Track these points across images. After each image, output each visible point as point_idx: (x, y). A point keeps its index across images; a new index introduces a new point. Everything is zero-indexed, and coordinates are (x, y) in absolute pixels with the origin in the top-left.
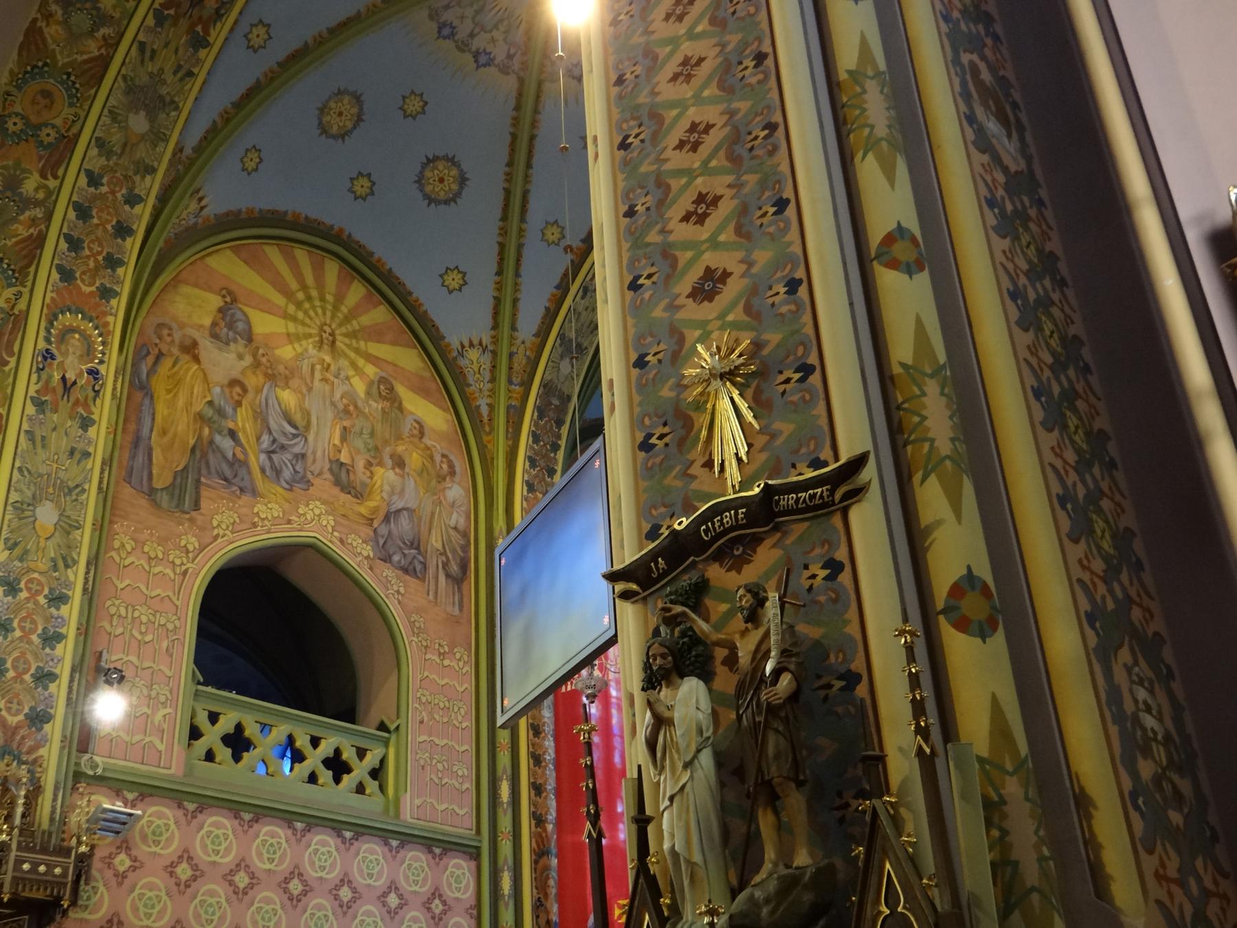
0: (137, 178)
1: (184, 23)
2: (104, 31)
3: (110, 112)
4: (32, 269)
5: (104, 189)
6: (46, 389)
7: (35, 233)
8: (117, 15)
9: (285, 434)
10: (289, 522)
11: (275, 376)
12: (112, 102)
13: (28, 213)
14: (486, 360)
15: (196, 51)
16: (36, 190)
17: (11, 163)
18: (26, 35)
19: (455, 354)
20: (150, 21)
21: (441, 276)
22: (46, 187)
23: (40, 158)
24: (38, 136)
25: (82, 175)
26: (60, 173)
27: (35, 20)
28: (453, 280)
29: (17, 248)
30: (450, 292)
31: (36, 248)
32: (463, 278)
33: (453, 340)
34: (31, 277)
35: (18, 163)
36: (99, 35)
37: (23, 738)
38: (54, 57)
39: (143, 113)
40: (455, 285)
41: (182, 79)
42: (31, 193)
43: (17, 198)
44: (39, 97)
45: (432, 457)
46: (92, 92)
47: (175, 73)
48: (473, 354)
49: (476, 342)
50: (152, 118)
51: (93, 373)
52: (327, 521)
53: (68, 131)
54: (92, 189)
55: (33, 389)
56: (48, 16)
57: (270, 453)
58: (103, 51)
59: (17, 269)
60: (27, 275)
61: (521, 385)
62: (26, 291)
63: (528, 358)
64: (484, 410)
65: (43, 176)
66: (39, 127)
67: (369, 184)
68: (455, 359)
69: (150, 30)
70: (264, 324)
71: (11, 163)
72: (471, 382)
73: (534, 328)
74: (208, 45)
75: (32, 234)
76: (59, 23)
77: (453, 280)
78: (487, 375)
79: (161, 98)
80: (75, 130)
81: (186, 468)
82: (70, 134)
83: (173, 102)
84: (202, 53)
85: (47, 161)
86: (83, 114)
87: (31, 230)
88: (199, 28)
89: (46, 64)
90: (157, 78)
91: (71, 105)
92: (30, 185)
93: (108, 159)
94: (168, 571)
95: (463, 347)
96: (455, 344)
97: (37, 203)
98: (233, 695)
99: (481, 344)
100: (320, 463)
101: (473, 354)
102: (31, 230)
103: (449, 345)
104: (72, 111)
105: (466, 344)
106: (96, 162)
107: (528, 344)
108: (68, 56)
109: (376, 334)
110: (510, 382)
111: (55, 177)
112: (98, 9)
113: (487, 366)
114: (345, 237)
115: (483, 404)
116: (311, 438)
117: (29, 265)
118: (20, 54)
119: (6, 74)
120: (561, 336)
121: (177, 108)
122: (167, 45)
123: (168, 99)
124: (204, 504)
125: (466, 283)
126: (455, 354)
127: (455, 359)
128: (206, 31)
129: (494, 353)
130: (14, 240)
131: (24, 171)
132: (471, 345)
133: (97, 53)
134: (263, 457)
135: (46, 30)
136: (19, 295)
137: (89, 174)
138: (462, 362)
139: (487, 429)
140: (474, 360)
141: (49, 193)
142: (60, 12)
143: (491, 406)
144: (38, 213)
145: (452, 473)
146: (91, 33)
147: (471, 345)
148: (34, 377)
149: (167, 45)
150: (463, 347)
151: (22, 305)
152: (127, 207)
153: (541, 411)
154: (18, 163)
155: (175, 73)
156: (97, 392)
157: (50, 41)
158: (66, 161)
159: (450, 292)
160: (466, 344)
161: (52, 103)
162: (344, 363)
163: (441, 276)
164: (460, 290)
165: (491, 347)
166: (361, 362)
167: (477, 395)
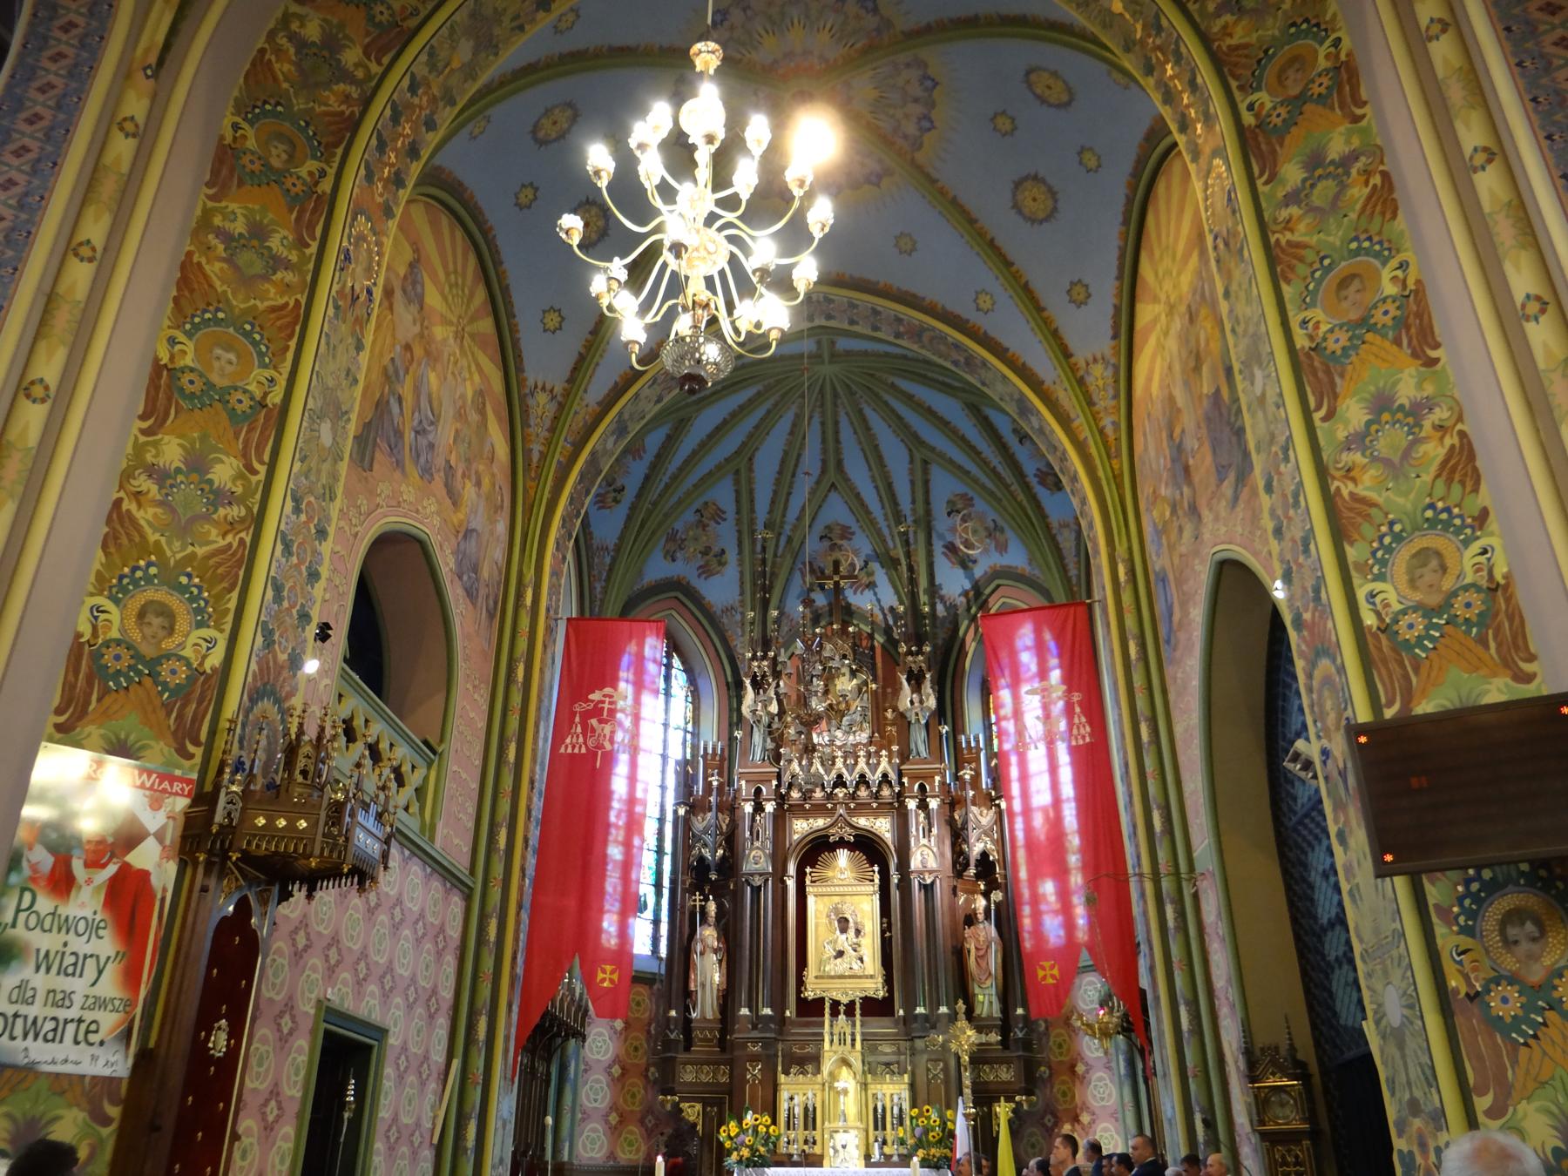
0: (441, 104)
3: (452, 26)
4: (340, 151)
6: (341, 293)
7: (347, 113)
9: (427, 418)
10: (417, 512)
11: (432, 356)
12: (457, 17)
14: (553, 407)
15: (537, 10)
16: (357, 65)
17: (335, 21)
19: (527, 391)
21: (544, 312)
23: (368, 34)
24: (371, 9)
25: (408, 77)
26: (386, 60)
28: (552, 320)
30: (545, 331)
32: (560, 323)
33: (532, 376)
34: (338, 159)
37: (284, 681)
39: (472, 43)
40: (551, 325)
41: (513, 29)
42: (350, 66)
43: (334, 63)
45: (494, 485)
48: (542, 398)
49: (548, 387)
50: (476, 52)
51: (369, 292)
52: (436, 521)
53: (403, 20)
54: (409, 95)
55: (336, 287)
57: (417, 432)
59: (324, 141)
60: (334, 155)
61: (573, 444)
62: (331, 172)
63: (586, 422)
64: (535, 457)
65: (367, 54)
67: (531, 197)
68: (526, 395)
70: (433, 298)
71: (335, 21)
72: (532, 423)
73: (600, 397)
75: (343, 113)
77: (552, 320)
78: (548, 423)
80: (412, 23)
81: (370, 422)
83: (497, 46)
84: (541, 14)
87: (343, 107)
92: (351, 56)
93: (430, 72)
94: (347, 528)
95: (536, 387)
96: (530, 382)
97: (352, 80)
98: (357, 678)
99: (551, 391)
100: (440, 462)
101: (542, 398)
102: (343, 107)
103: (525, 380)
105: (540, 385)
106: (421, 70)
107: (590, 409)
109: (483, 346)
110: (566, 440)
111: (379, 63)
113: (550, 415)
114: (490, 237)
115: (536, 448)
116: (440, 429)
117: (337, 145)
120: (620, 413)
121: (496, 54)
123: (494, 42)
124: (376, 466)
125: (560, 328)
126: (527, 391)
127: (526, 395)
129: (561, 406)
130: (323, 108)
131: (346, 37)
132: (543, 389)
134: (413, 434)
136: (323, 174)
137: (413, 76)
138: (531, 402)
139: (533, 475)
140: (542, 405)
141: (369, 77)
143: (543, 456)
144: (354, 92)
145: (502, 507)
147: (543, 389)
148: (337, 274)
150: (536, 387)
151: (326, 186)
152: (424, 129)
153: (582, 475)
155: (512, 20)
156: (369, 315)
159: (545, 331)
160: (540, 385)
162: (464, 362)
163: (544, 312)
164: (554, 332)
165: (559, 398)
166: (473, 368)
167: (533, 438)
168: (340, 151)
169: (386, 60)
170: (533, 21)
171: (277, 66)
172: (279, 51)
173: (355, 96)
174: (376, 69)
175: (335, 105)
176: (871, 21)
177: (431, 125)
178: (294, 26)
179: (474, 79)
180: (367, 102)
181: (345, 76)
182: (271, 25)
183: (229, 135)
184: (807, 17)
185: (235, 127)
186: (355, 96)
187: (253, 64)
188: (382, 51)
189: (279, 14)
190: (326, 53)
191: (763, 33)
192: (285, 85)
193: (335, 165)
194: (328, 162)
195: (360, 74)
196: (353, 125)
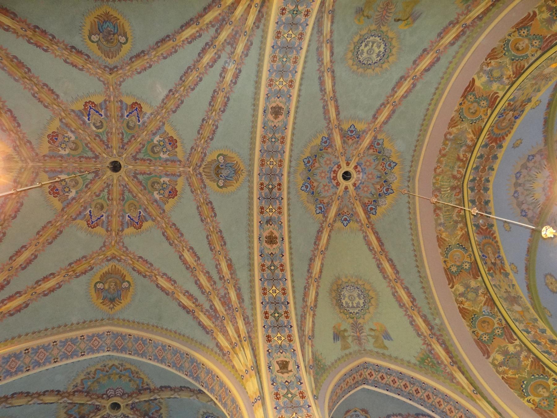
0: (536, 324)
1: (497, 272)
2: (480, 292)
4: (547, 369)
5: (533, 333)
8: (479, 285)
12: (505, 307)
13: (522, 357)
15: (508, 278)
16: (515, 348)
17: (498, 348)
18: (461, 312)
20: (490, 278)
22: (516, 345)
23: (504, 339)
25: (523, 332)
26: (515, 337)
27: (459, 307)
29: (533, 368)
31: (539, 363)
34: (550, 372)
35: (500, 347)
36: (480, 294)
38: (474, 311)
39: (515, 304)
41: (513, 288)
44: (483, 325)
46: (496, 309)
47: (510, 287)
56: (462, 303)
58: (486, 297)
59: (541, 373)
60: (548, 372)
66: (493, 331)
69: (493, 280)
71: (498, 348)
74: (509, 274)
75: (532, 361)
76: (466, 301)
79: (514, 297)
82: (504, 326)
84: (510, 277)
85: (507, 339)
86: (501, 317)
87: (530, 360)
88: (502, 271)
89: (475, 315)
90: (507, 292)
91: (494, 318)
92: (511, 349)
93: (523, 323)
97: (520, 352)
102: (530, 360)
104: (497, 319)
106: (522, 326)
108: (478, 307)
111: (516, 340)
112: (473, 288)
117: (544, 369)
118: (465, 319)
119: (467, 327)
121: (521, 297)
122: (500, 281)
128: (505, 270)
130: (529, 367)
133: (485, 299)
135: (464, 307)
142: (463, 299)
144: (524, 353)
146: (477, 295)
149: (500, 281)
154: (500, 347)
157: (469, 308)
158: (513, 333)
161: (488, 322)
168: (547, 369)
169: (515, 337)
170: (512, 281)
171: (509, 376)
172: (504, 372)
173: (526, 354)
174: (517, 342)
175: (529, 362)
176: (538, 158)
177: (544, 331)
178: (497, 363)
179: (529, 309)
180: (529, 350)
181: (517, 355)
182: (495, 370)
183: (530, 405)
184: (530, 181)
185: (529, 401)
186: (526, 354)
187: (507, 383)
188: (512, 337)
189: (491, 366)
190: (508, 357)
191: (533, 198)
192: (517, 376)
193: (552, 373)
194: (550, 376)
195: (518, 348)
196: (537, 359)
